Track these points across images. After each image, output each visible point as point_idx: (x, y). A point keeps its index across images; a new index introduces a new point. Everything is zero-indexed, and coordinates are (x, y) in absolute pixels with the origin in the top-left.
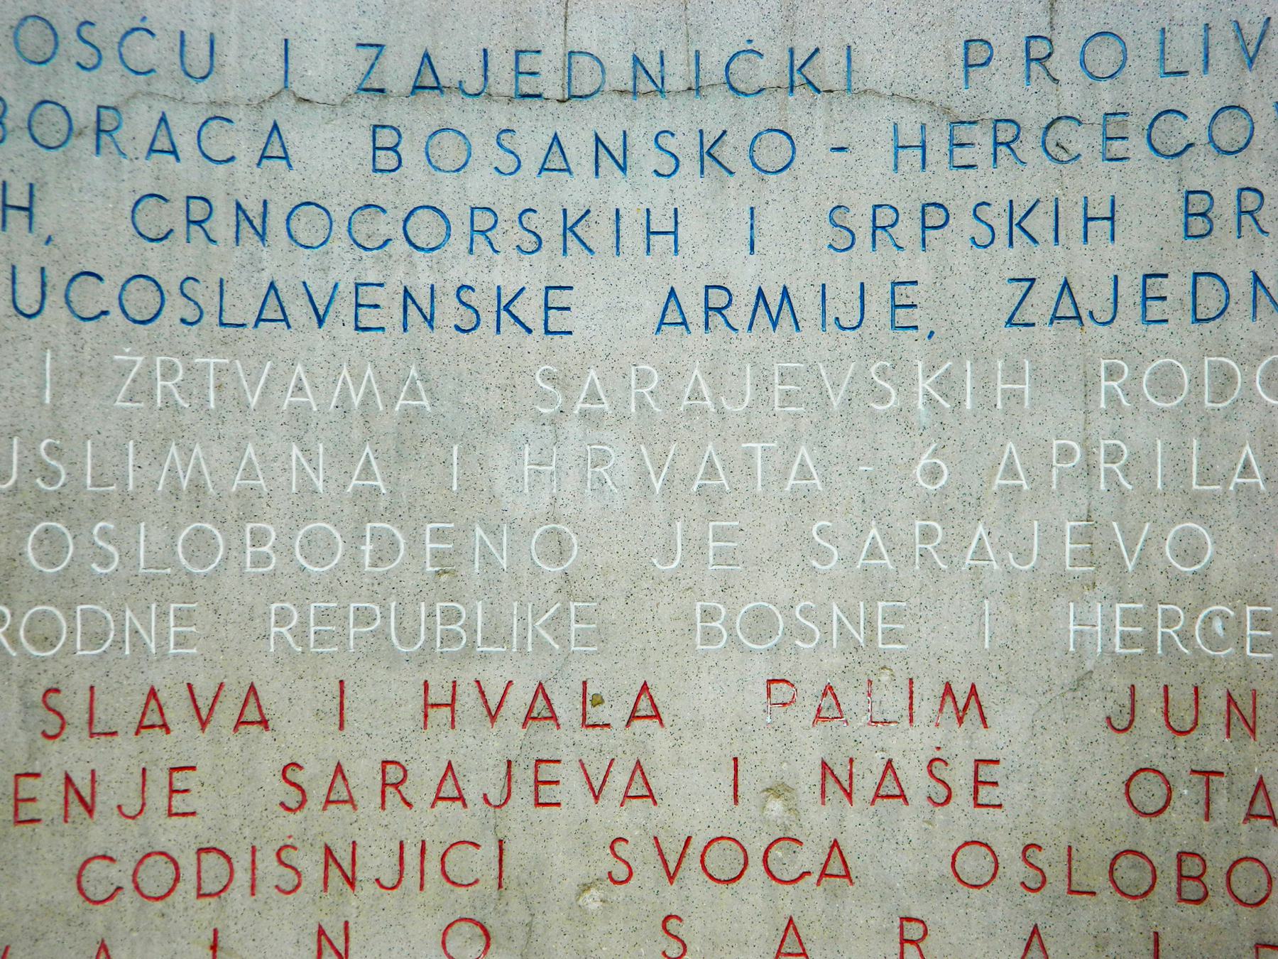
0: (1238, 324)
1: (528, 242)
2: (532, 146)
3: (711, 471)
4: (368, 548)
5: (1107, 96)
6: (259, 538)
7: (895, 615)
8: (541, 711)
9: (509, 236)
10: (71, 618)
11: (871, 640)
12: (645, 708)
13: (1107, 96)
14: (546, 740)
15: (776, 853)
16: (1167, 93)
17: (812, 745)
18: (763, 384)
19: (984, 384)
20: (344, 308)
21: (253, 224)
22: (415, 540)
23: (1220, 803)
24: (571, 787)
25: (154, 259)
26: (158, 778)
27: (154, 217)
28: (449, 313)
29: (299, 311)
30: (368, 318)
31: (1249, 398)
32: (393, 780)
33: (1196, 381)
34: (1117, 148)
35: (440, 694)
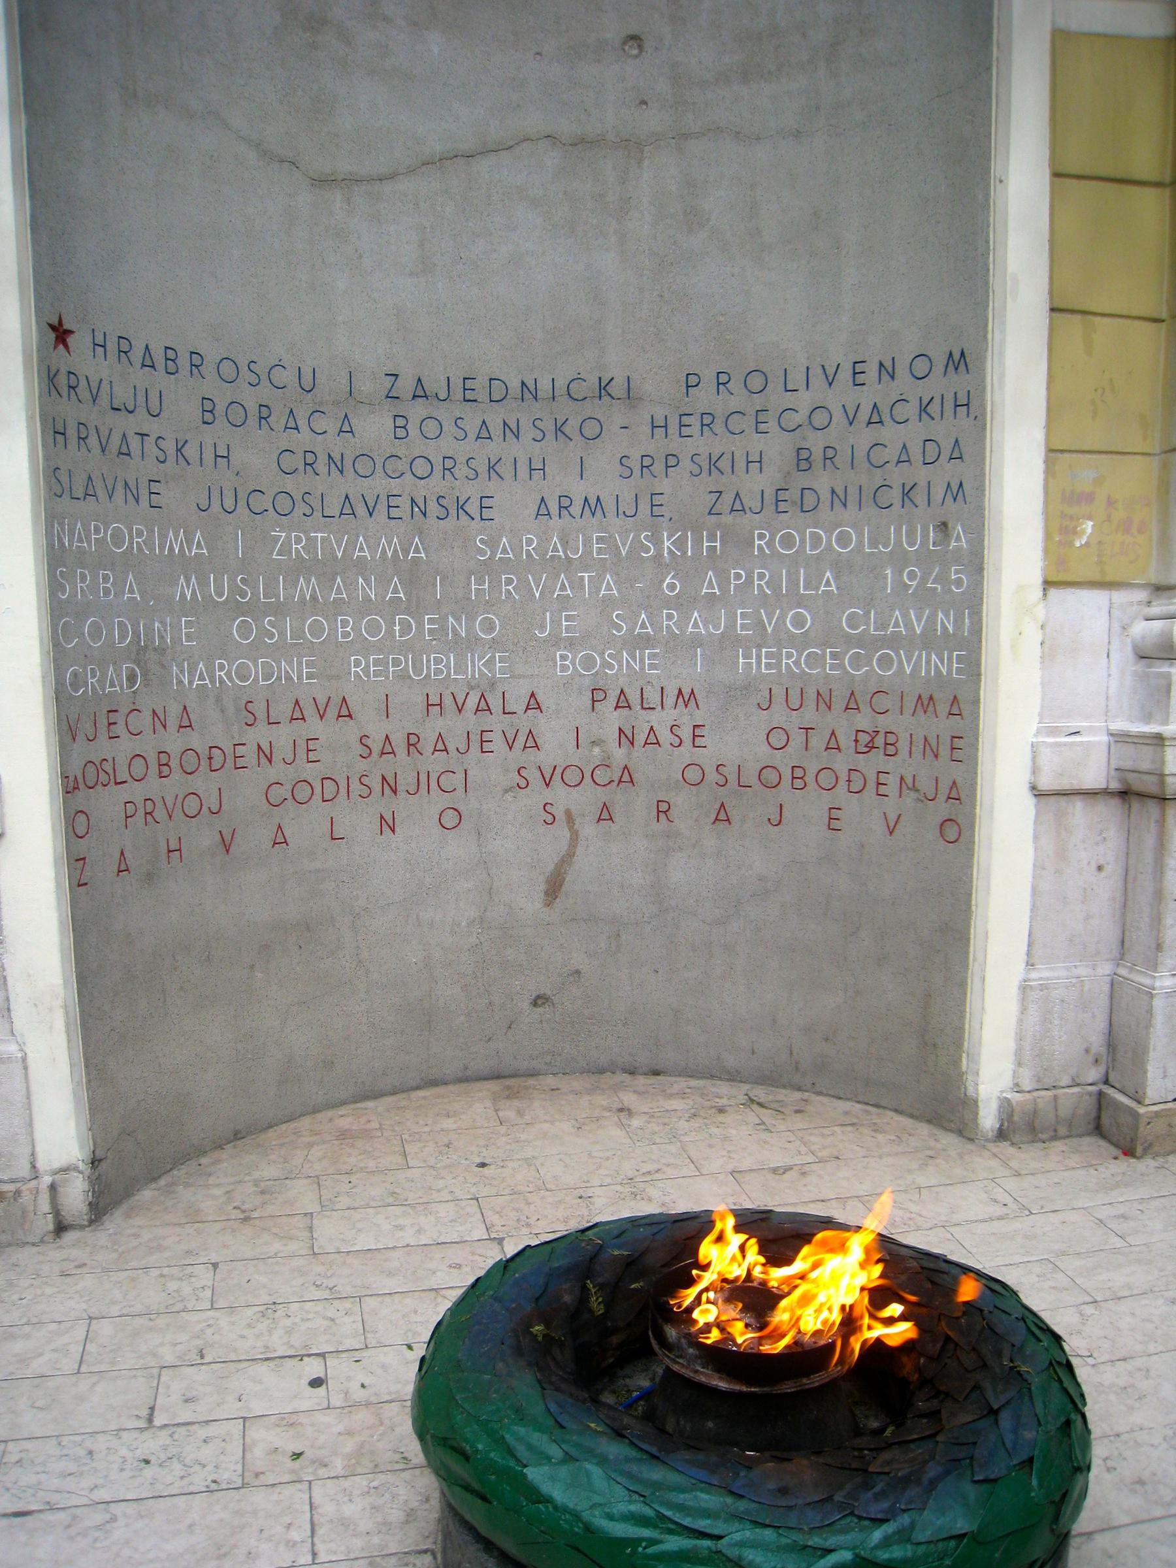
0: (824, 512)
1: (472, 475)
2: (472, 425)
3: (563, 588)
4: (397, 628)
5: (758, 401)
6: (345, 623)
7: (653, 656)
8: (483, 708)
9: (461, 471)
10: (256, 666)
11: (642, 668)
12: (534, 703)
13: (758, 401)
14: (488, 721)
15: (597, 772)
16: (789, 400)
17: (613, 719)
18: (587, 543)
19: (698, 542)
20: (382, 507)
21: (337, 464)
22: (420, 624)
23: (813, 742)
24: (498, 744)
25: (289, 483)
26: (301, 744)
27: (288, 462)
28: (433, 507)
29: (361, 511)
30: (394, 513)
31: (829, 547)
32: (412, 743)
33: (803, 541)
34: (762, 427)
35: (434, 699)
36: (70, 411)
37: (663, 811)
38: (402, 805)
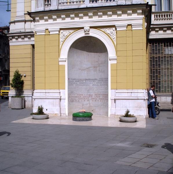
8: (90, 95)
21: (82, 83)
36: (69, 82)
37: (98, 101)
38: (85, 100)
